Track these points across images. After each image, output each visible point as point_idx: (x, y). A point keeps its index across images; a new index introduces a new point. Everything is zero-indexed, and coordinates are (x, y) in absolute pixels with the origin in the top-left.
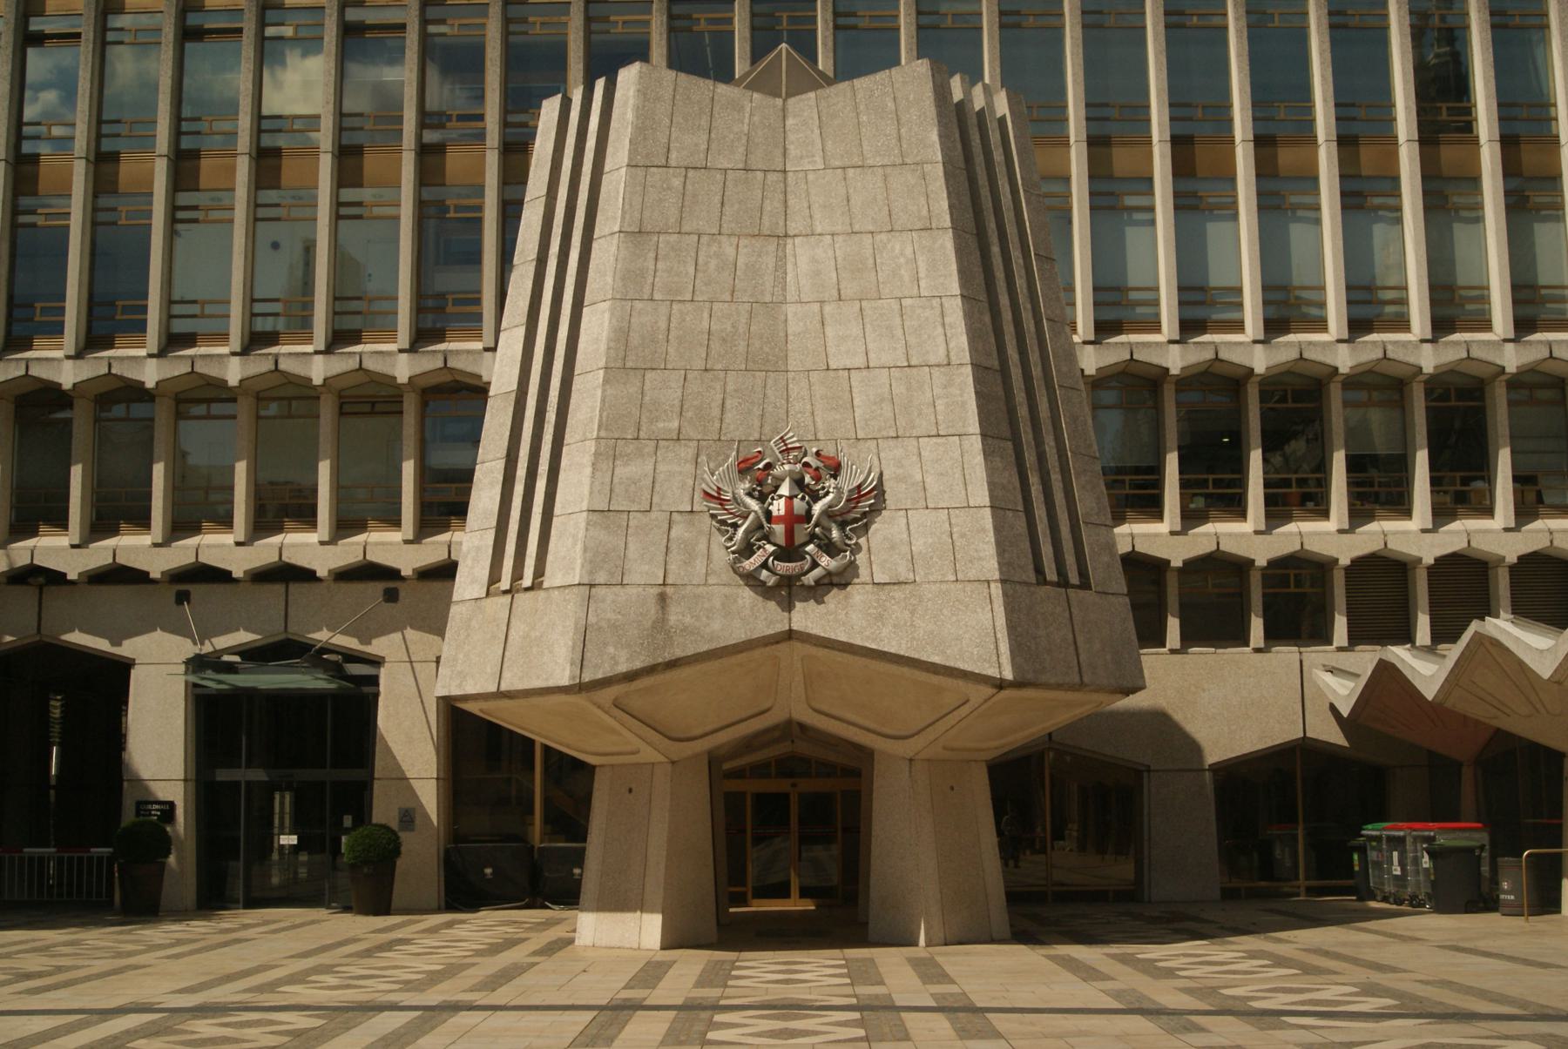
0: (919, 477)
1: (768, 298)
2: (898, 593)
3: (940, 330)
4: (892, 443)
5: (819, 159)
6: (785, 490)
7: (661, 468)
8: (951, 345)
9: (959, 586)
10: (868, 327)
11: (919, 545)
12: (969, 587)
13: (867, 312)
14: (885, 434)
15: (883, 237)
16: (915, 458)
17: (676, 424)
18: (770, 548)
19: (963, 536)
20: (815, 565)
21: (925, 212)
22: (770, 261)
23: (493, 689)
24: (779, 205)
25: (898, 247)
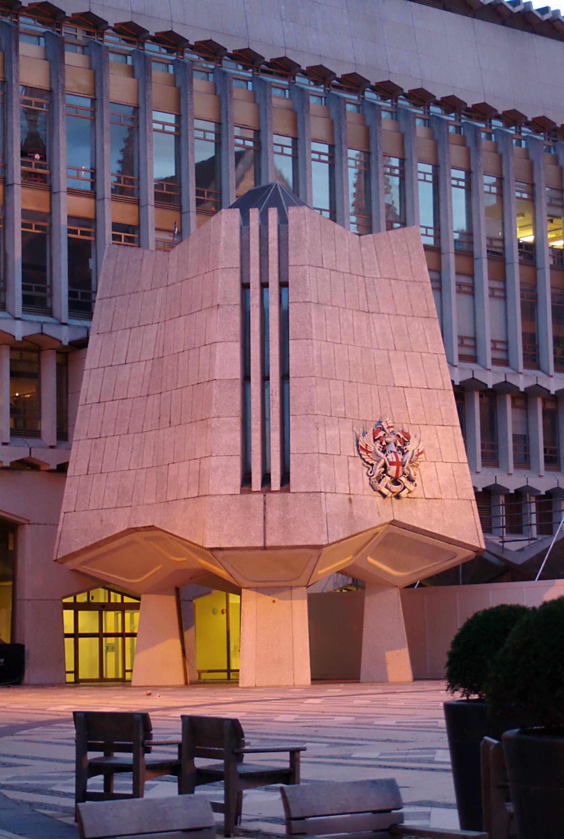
0: (438, 446)
1: (366, 346)
2: (436, 503)
3: (439, 371)
4: (425, 427)
5: (377, 272)
6: (392, 448)
7: (342, 433)
8: (444, 380)
9: (460, 501)
10: (409, 365)
11: (441, 480)
12: (464, 502)
13: (408, 358)
14: (421, 422)
15: (409, 319)
16: (435, 436)
17: (343, 410)
18: (388, 478)
19: (458, 477)
20: (405, 488)
21: (426, 309)
22: (364, 326)
23: (261, 544)
24: (364, 294)
25: (417, 325)
